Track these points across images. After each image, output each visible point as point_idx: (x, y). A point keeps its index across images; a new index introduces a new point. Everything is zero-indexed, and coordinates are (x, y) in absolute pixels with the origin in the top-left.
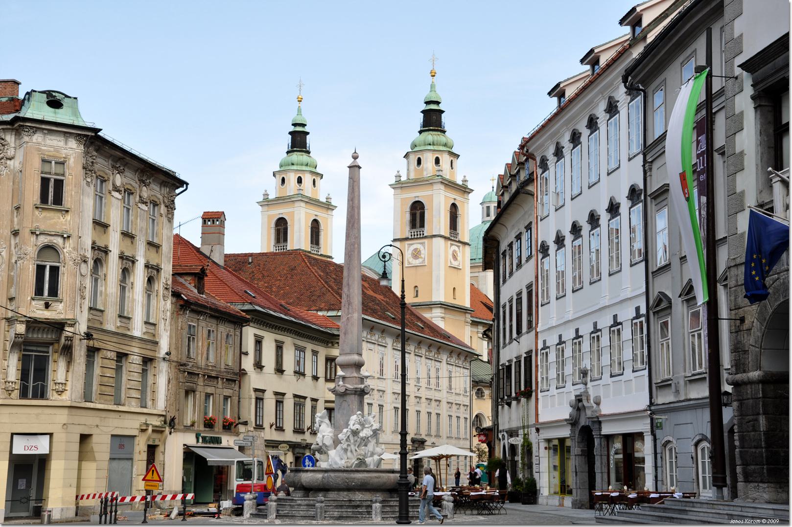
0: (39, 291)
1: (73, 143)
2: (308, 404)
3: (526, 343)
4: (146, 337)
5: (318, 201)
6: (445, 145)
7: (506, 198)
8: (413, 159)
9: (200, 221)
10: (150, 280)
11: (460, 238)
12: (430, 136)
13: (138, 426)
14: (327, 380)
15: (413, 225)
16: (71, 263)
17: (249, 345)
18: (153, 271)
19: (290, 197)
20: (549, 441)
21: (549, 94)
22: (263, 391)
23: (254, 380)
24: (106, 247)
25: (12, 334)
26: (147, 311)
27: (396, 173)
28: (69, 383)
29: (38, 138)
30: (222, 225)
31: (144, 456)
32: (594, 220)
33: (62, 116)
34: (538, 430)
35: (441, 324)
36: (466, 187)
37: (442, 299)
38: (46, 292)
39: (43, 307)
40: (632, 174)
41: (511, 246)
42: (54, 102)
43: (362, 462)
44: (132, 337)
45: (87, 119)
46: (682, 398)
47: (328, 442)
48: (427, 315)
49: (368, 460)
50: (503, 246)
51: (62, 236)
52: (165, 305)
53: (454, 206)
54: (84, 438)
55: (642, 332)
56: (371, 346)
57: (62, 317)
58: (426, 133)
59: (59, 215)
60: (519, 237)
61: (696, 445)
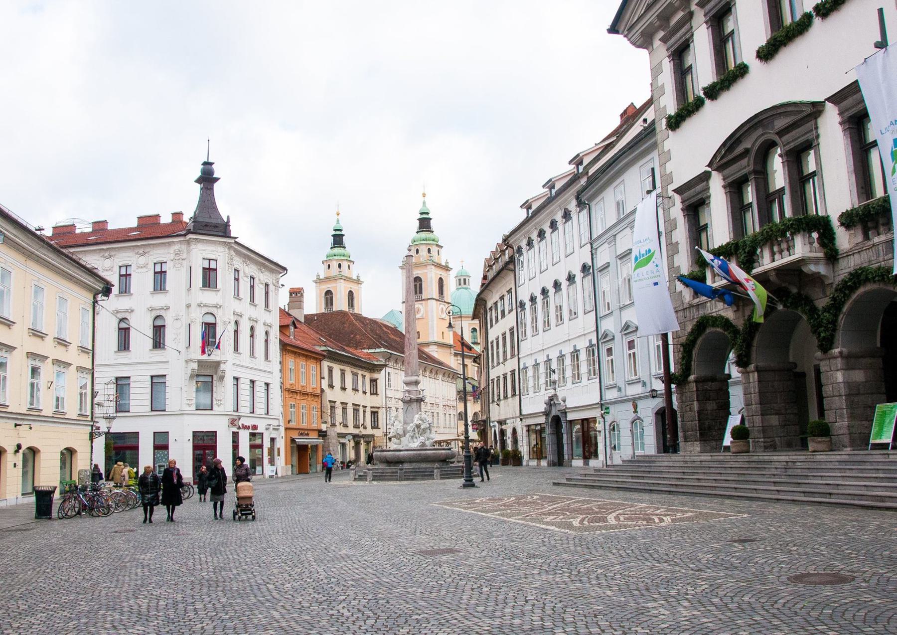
2: (361, 410)
3: (512, 364)
5: (351, 279)
6: (434, 240)
9: (288, 294)
12: (424, 235)
17: (326, 373)
20: (528, 426)
22: (335, 402)
23: (329, 395)
30: (302, 295)
32: (557, 285)
34: (521, 420)
35: (436, 355)
37: (436, 340)
41: (496, 303)
43: (423, 444)
48: (426, 350)
49: (427, 443)
50: (490, 304)
53: (441, 279)
55: (593, 355)
60: (502, 298)
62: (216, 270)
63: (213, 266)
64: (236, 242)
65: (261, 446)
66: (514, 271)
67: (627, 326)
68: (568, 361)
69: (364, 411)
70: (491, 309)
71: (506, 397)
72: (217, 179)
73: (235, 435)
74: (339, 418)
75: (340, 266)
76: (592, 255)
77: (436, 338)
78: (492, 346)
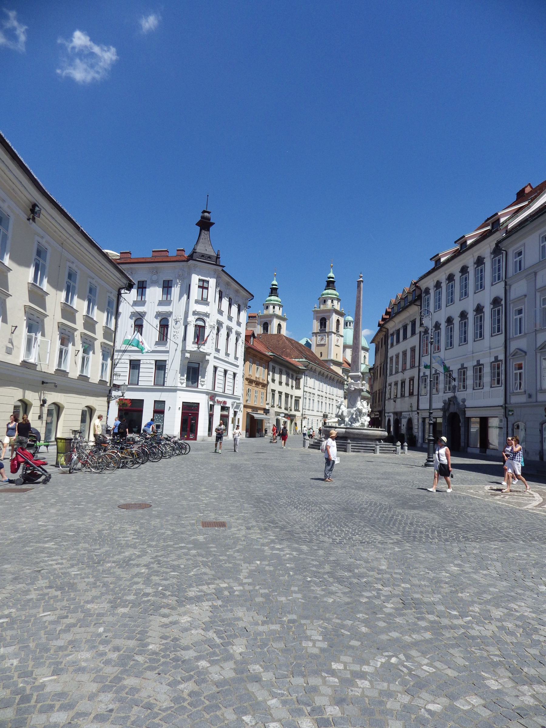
11: (340, 333)
15: (321, 327)
18: (238, 334)
21: (431, 259)
34: (418, 413)
53: (338, 321)
62: (207, 288)
63: (205, 285)
64: (223, 270)
65: (227, 416)
66: (421, 306)
68: (470, 373)
70: (392, 335)
71: (403, 396)
72: (213, 224)
73: (211, 408)
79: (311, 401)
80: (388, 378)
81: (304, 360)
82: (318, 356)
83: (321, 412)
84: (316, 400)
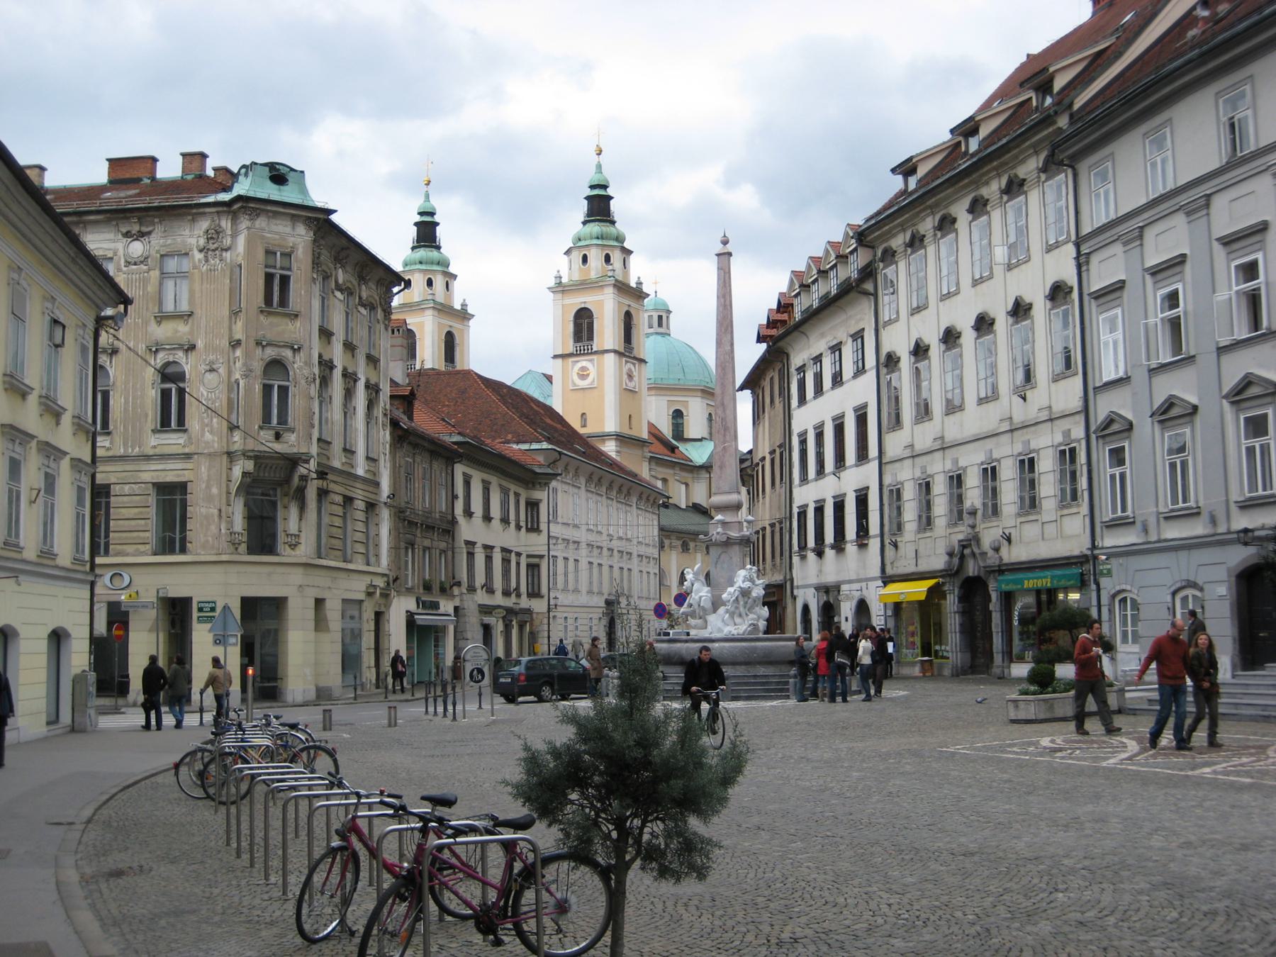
0: (267, 418)
1: (301, 229)
4: (367, 476)
7: (813, 299)
8: (577, 256)
10: (371, 405)
12: (595, 228)
13: (364, 589)
14: (528, 530)
15: (578, 336)
16: (303, 382)
17: (460, 490)
19: (419, 303)
21: (893, 171)
22: (473, 544)
23: (469, 530)
24: (331, 361)
25: (237, 472)
26: (365, 443)
27: (555, 273)
28: (303, 535)
29: (261, 222)
31: (372, 626)
33: (287, 194)
36: (641, 291)
38: (275, 420)
39: (272, 438)
40: (1063, 267)
42: (278, 175)
44: (356, 477)
45: (319, 198)
46: (1153, 538)
47: (706, 603)
51: (292, 348)
52: (385, 435)
53: (628, 315)
54: (319, 603)
56: (566, 487)
57: (295, 450)
58: (592, 224)
59: (287, 320)
60: (836, 348)
61: (1174, 594)
66: (876, 295)
67: (1170, 404)
69: (518, 564)
70: (802, 369)
74: (480, 579)
75: (430, 283)
76: (1079, 267)
77: (611, 426)
78: (803, 442)
79: (571, 563)
80: (796, 491)
81: (545, 445)
82: (575, 424)
83: (600, 593)
84: (583, 564)
